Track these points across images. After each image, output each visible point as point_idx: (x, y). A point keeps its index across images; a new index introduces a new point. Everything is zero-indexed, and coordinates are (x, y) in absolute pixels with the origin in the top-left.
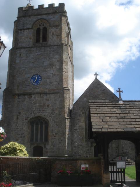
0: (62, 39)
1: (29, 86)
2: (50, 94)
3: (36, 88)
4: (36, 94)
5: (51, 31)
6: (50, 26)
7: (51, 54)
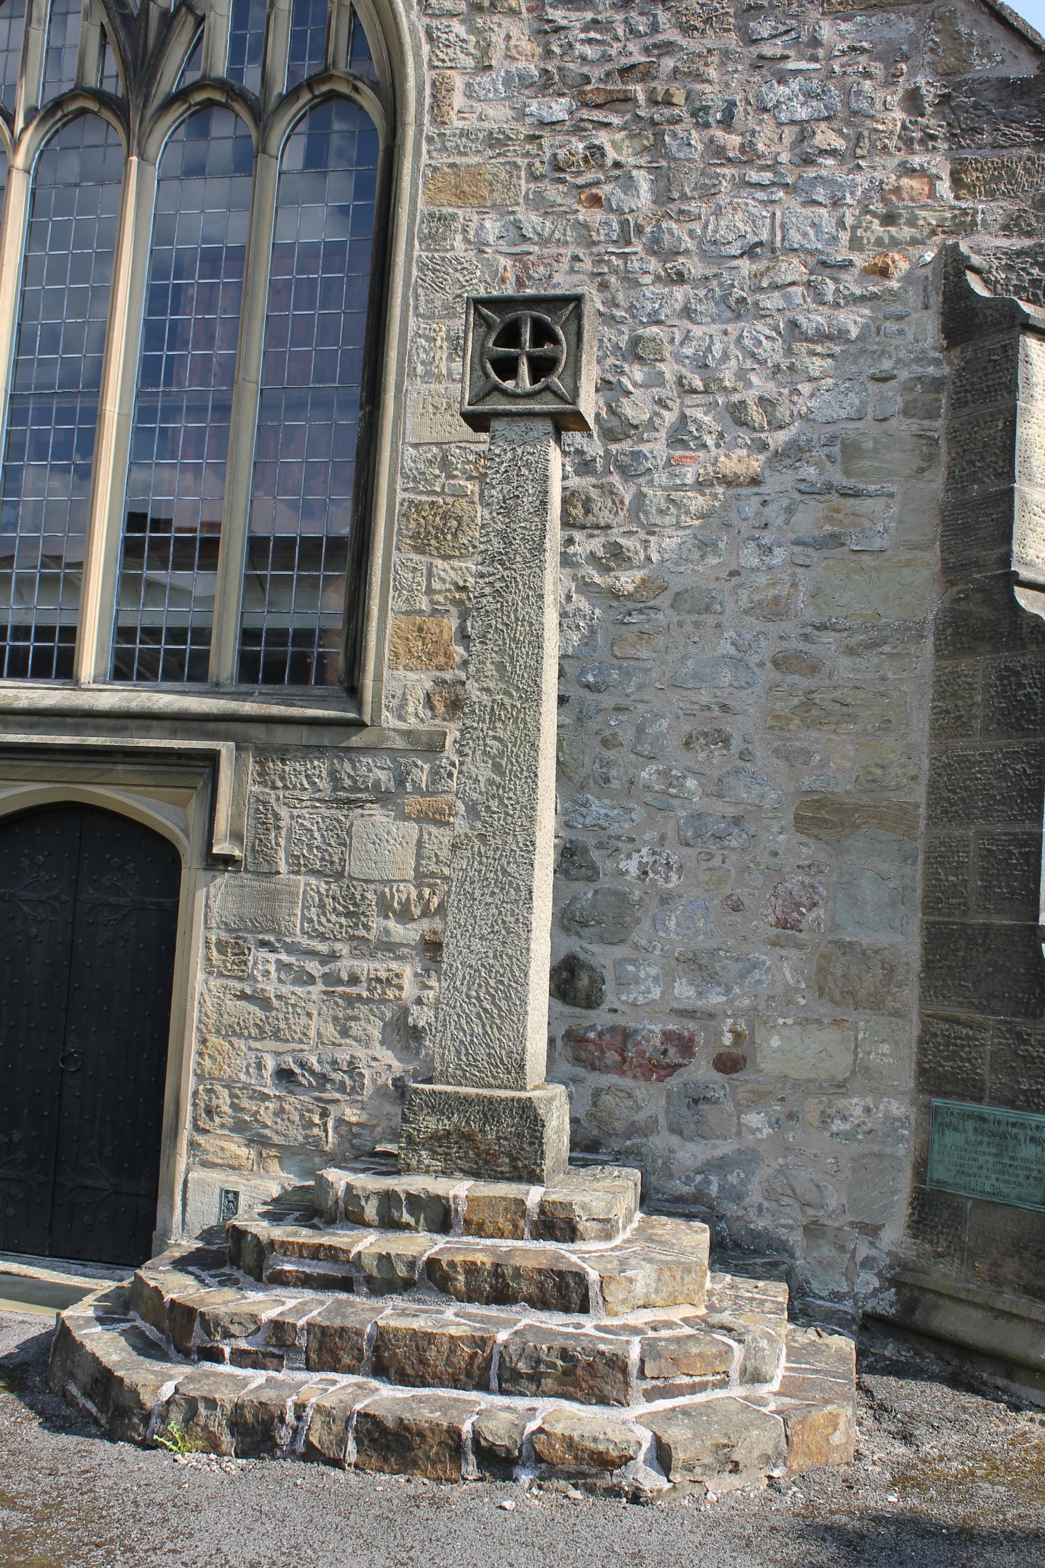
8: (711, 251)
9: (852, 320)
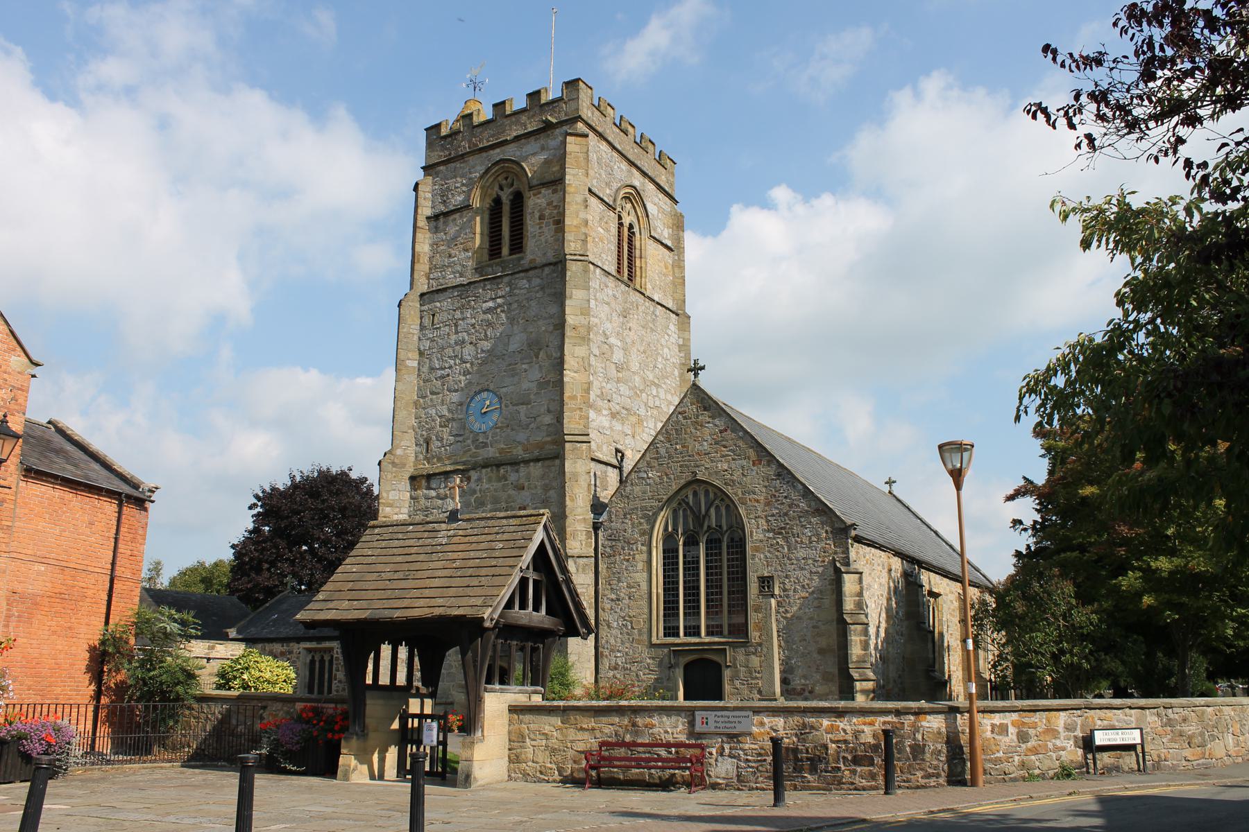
0: (568, 236)
1: (460, 439)
2: (526, 462)
3: (485, 445)
4: (484, 467)
5: (535, 203)
6: (531, 188)
7: (533, 303)
8: (797, 559)
9: (820, 570)
